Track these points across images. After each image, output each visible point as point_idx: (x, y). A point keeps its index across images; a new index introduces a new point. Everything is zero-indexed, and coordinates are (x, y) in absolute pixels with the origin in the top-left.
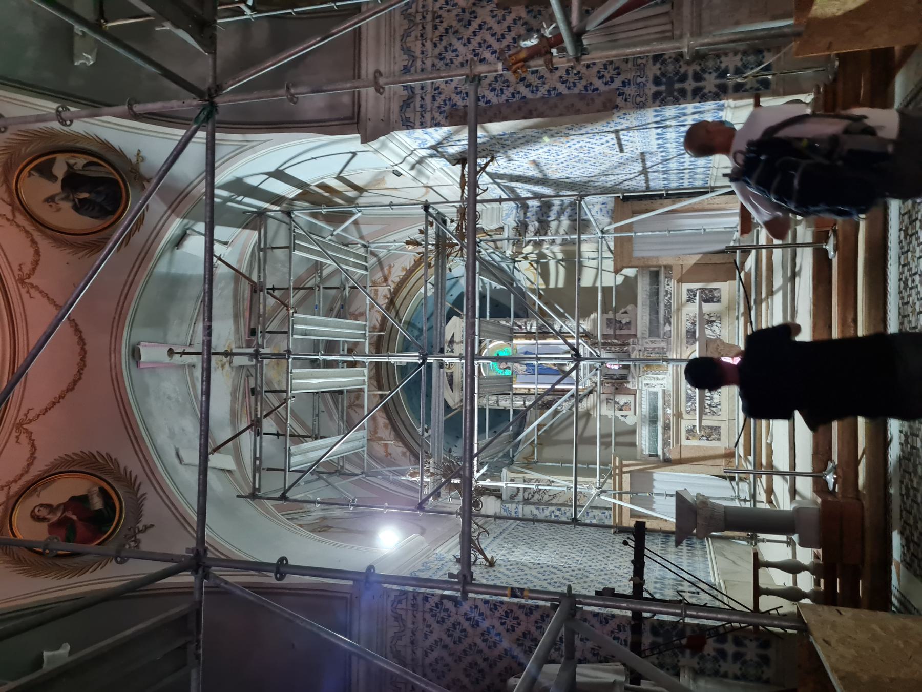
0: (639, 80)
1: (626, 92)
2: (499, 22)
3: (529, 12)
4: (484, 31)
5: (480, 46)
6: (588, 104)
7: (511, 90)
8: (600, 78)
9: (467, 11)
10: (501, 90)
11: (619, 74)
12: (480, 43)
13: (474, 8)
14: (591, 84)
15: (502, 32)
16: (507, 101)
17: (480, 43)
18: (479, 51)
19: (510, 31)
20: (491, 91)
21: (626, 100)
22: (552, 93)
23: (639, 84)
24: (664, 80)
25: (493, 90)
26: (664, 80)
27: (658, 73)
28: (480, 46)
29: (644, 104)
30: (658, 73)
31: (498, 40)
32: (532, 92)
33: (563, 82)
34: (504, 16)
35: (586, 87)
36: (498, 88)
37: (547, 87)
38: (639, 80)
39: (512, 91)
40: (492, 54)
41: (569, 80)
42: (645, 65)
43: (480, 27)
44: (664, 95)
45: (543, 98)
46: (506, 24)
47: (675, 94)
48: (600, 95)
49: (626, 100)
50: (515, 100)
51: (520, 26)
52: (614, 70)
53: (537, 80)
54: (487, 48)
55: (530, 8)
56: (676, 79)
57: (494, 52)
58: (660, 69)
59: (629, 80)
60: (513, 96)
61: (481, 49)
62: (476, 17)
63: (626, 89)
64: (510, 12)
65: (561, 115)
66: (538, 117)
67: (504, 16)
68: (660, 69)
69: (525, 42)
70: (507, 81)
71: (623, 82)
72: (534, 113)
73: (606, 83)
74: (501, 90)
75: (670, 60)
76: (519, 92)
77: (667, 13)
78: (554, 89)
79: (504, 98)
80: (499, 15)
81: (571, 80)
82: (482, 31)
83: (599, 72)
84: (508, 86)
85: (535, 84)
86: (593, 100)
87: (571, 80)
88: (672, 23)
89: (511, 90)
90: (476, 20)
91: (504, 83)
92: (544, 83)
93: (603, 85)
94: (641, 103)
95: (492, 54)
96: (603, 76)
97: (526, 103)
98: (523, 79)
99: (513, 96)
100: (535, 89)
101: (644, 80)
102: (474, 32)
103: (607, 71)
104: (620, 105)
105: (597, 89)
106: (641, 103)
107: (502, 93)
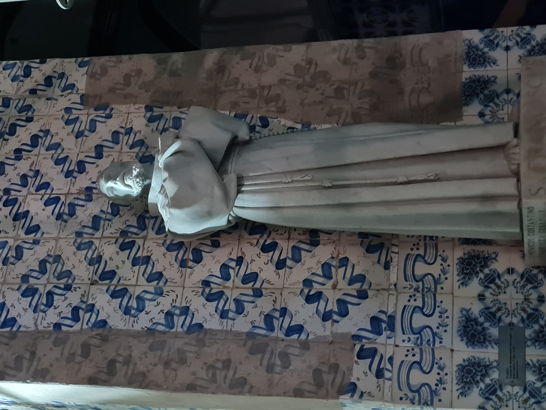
0: (419, 320)
1: (381, 350)
2: (79, 135)
3: (151, 120)
4: (41, 150)
5: (24, 184)
6: (270, 369)
7: (74, 298)
8: (309, 299)
9: (13, 104)
10: (50, 294)
11: (363, 295)
12: (24, 177)
13: (29, 102)
14: (284, 311)
15: (81, 157)
16: (57, 326)
17: (24, 177)
18: (21, 194)
19: (99, 156)
20: (24, 295)
21: (379, 374)
22: (178, 321)
23: (419, 332)
24: (494, 332)
25: (30, 292)
26: (494, 332)
27: (476, 308)
28: (24, 184)
29: (434, 393)
30: (476, 308)
31: (69, 174)
32: (127, 311)
33: (210, 298)
34: (93, 122)
35: (269, 319)
36: (41, 289)
37: (166, 303)
38: (419, 320)
39: (76, 302)
40: (46, 204)
41: (227, 292)
42: (437, 282)
43: (35, 140)
44: (495, 375)
45: (150, 331)
46: (93, 140)
47: (530, 377)
48: (305, 346)
49: (379, 374)
50: (77, 327)
51: (126, 149)
52: (351, 282)
53: (142, 281)
54: (38, 189)
55: (157, 111)
56: (528, 332)
57: (54, 201)
58: (481, 297)
59: (392, 318)
60: (76, 318)
61: (25, 191)
62: (30, 120)
63: (382, 339)
64: (109, 117)
65: (191, 388)
66: (130, 384)
67: (93, 122)
68: (481, 297)
69: (110, 184)
70: (69, 274)
71: (375, 320)
72: (121, 370)
73: (326, 317)
74: (50, 294)
75: (510, 278)
76: (91, 308)
77: (501, 148)
78: (185, 311)
79: (52, 317)
80: (83, 118)
81: (232, 294)
82: (36, 151)
83: (307, 283)
84: (68, 288)
85: (138, 291)
86: (285, 357)
87: (232, 294)
88: (517, 174)
89: (74, 298)
90: (30, 125)
91: (59, 277)
92: (160, 293)
93: (318, 320)
94: (425, 391)
95: (46, 204)
96: (319, 295)
97: (104, 339)
98: (109, 275)
99: (76, 318)
100: (134, 303)
101: (433, 321)
102: (18, 151)
103: (330, 283)
104: (361, 386)
105: (299, 329)
106: (425, 391)
107: (50, 304)
